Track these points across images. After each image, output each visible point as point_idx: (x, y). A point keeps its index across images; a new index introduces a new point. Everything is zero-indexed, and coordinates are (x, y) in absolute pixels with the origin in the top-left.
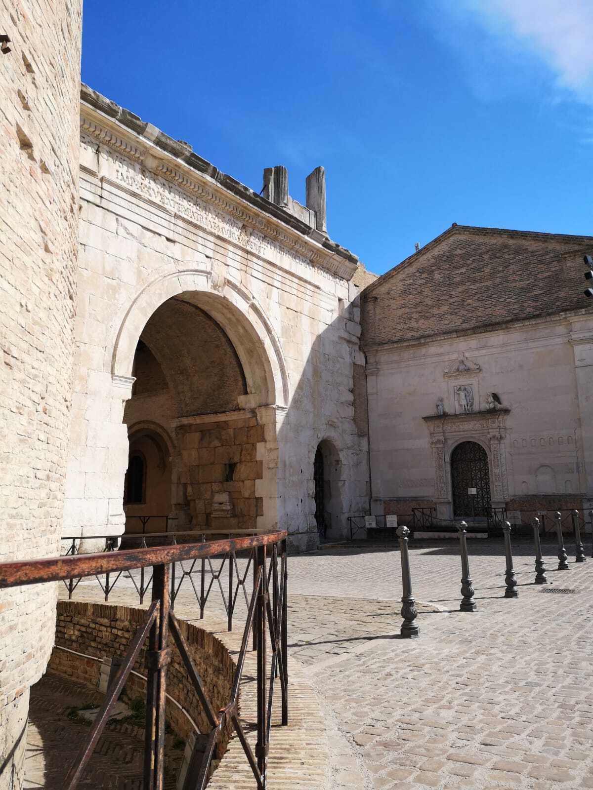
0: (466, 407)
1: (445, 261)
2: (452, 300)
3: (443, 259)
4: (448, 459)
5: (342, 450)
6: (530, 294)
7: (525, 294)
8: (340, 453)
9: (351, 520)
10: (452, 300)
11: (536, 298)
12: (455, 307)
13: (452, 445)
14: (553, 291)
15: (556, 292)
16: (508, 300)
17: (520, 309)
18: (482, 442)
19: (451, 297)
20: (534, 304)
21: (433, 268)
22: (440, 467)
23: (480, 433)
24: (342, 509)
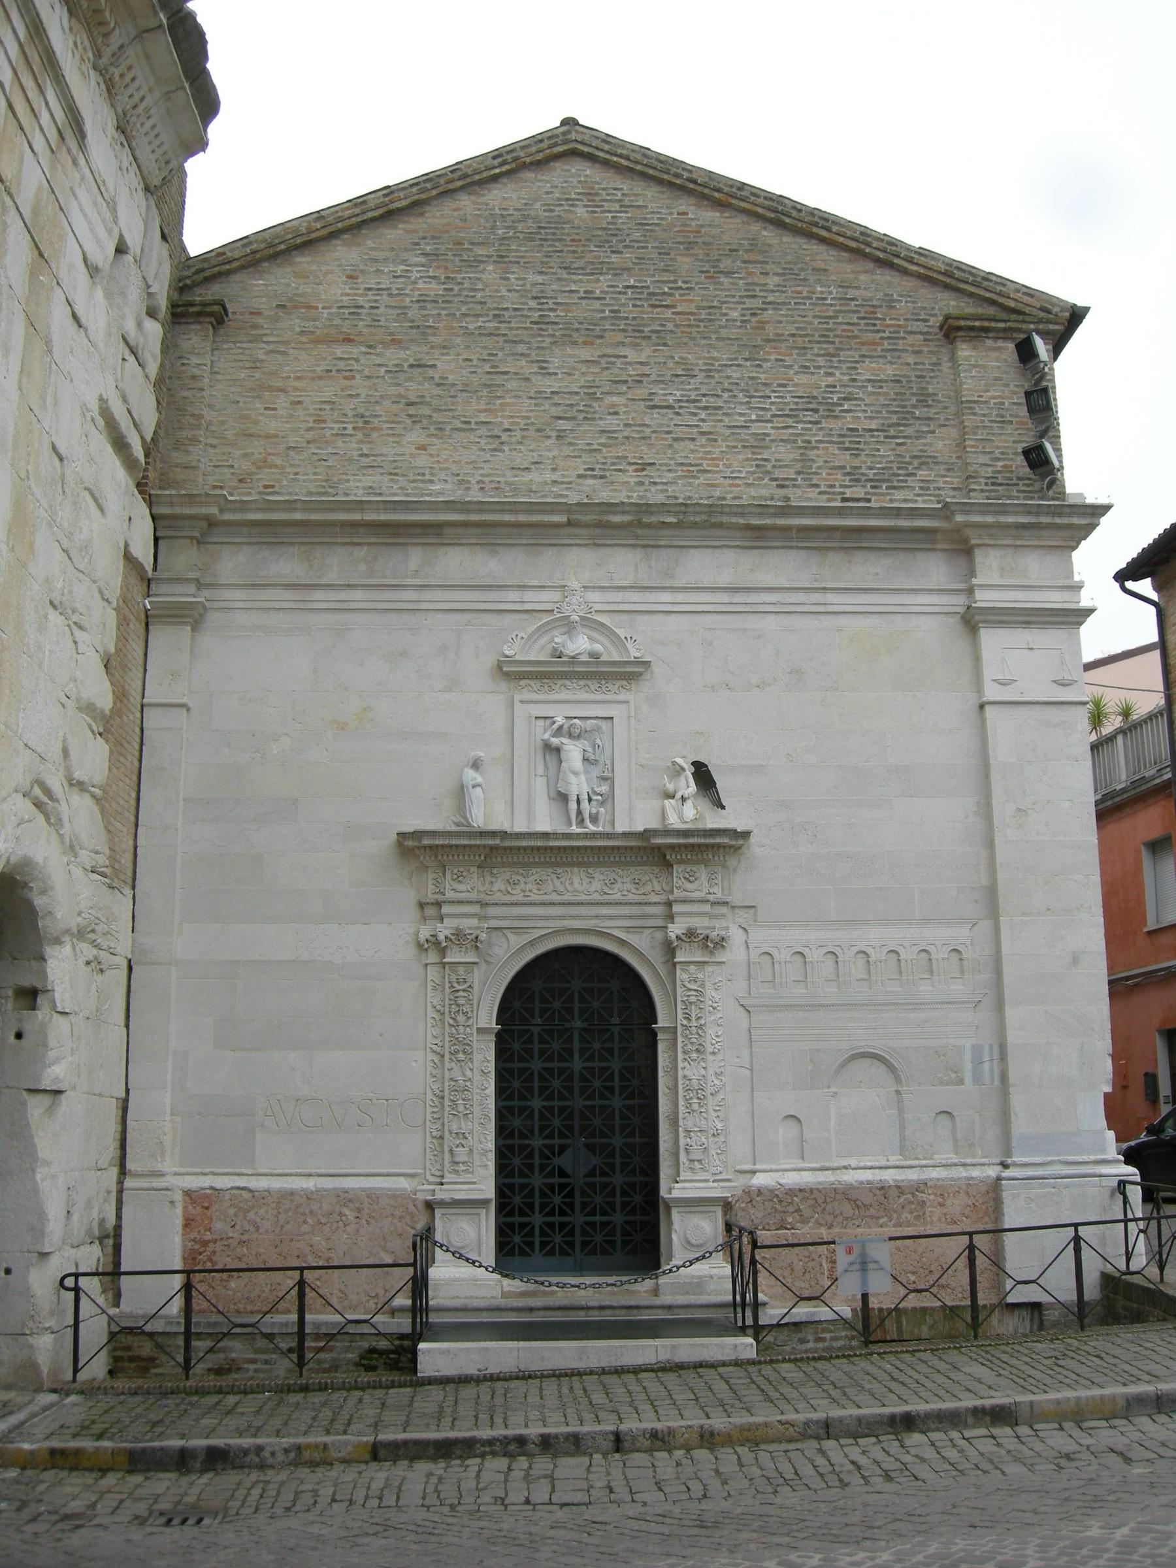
0: (585, 804)
1: (530, 238)
2: (547, 384)
3: (520, 226)
4: (487, 1016)
5: (58, 941)
6: (835, 425)
7: (816, 417)
8: (49, 951)
9: (77, 1290)
10: (547, 384)
11: (851, 441)
12: (555, 411)
13: (508, 956)
14: (910, 431)
15: (919, 436)
16: (757, 428)
17: (798, 466)
18: (639, 949)
19: (544, 372)
20: (845, 459)
21: (480, 251)
22: (462, 1049)
23: (631, 917)
24: (38, 1231)
